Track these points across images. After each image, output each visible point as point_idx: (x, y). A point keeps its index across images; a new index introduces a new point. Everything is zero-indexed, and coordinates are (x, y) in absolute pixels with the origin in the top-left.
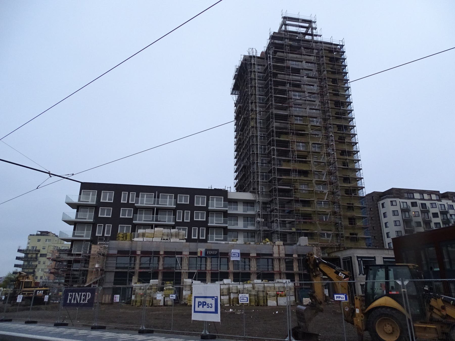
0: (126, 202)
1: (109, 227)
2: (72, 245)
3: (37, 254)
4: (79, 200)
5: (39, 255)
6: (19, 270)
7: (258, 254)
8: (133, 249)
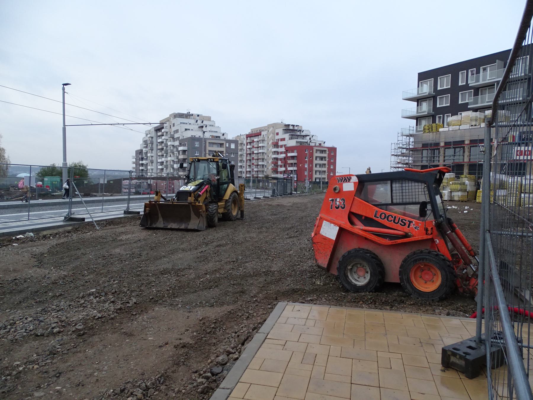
7: (471, 141)
8: (437, 141)
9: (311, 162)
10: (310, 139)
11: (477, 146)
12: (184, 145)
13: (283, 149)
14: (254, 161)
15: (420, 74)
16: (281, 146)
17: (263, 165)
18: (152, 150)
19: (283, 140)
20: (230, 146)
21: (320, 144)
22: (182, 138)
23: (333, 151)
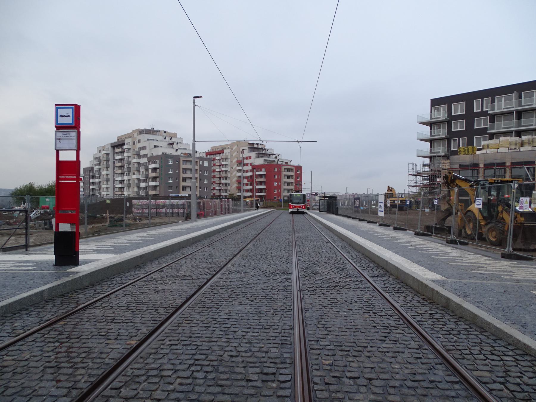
0: (480, 111)
1: (463, 140)
2: (430, 161)
4: (431, 118)
6: (426, 182)
8: (475, 162)
9: (279, 180)
10: (276, 157)
11: (522, 168)
12: (154, 163)
13: (250, 168)
14: (215, 179)
16: (247, 165)
17: (226, 184)
18: (107, 167)
19: (250, 158)
20: (203, 163)
21: (286, 163)
22: (151, 155)
23: (299, 169)
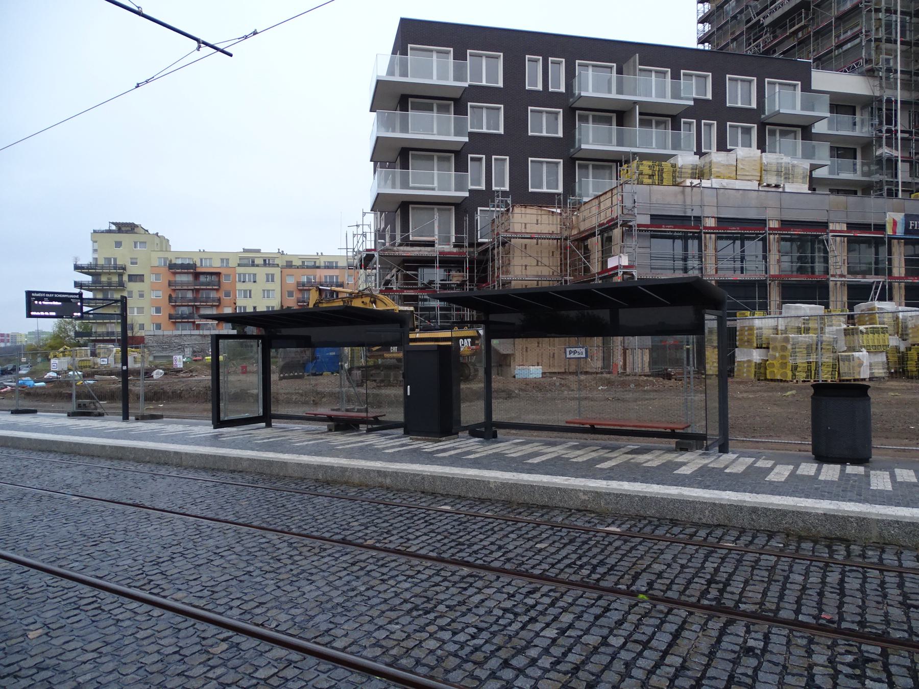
3: (121, 275)
5: (125, 278)
15: (405, 24)
